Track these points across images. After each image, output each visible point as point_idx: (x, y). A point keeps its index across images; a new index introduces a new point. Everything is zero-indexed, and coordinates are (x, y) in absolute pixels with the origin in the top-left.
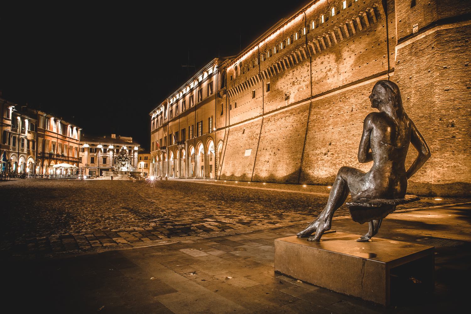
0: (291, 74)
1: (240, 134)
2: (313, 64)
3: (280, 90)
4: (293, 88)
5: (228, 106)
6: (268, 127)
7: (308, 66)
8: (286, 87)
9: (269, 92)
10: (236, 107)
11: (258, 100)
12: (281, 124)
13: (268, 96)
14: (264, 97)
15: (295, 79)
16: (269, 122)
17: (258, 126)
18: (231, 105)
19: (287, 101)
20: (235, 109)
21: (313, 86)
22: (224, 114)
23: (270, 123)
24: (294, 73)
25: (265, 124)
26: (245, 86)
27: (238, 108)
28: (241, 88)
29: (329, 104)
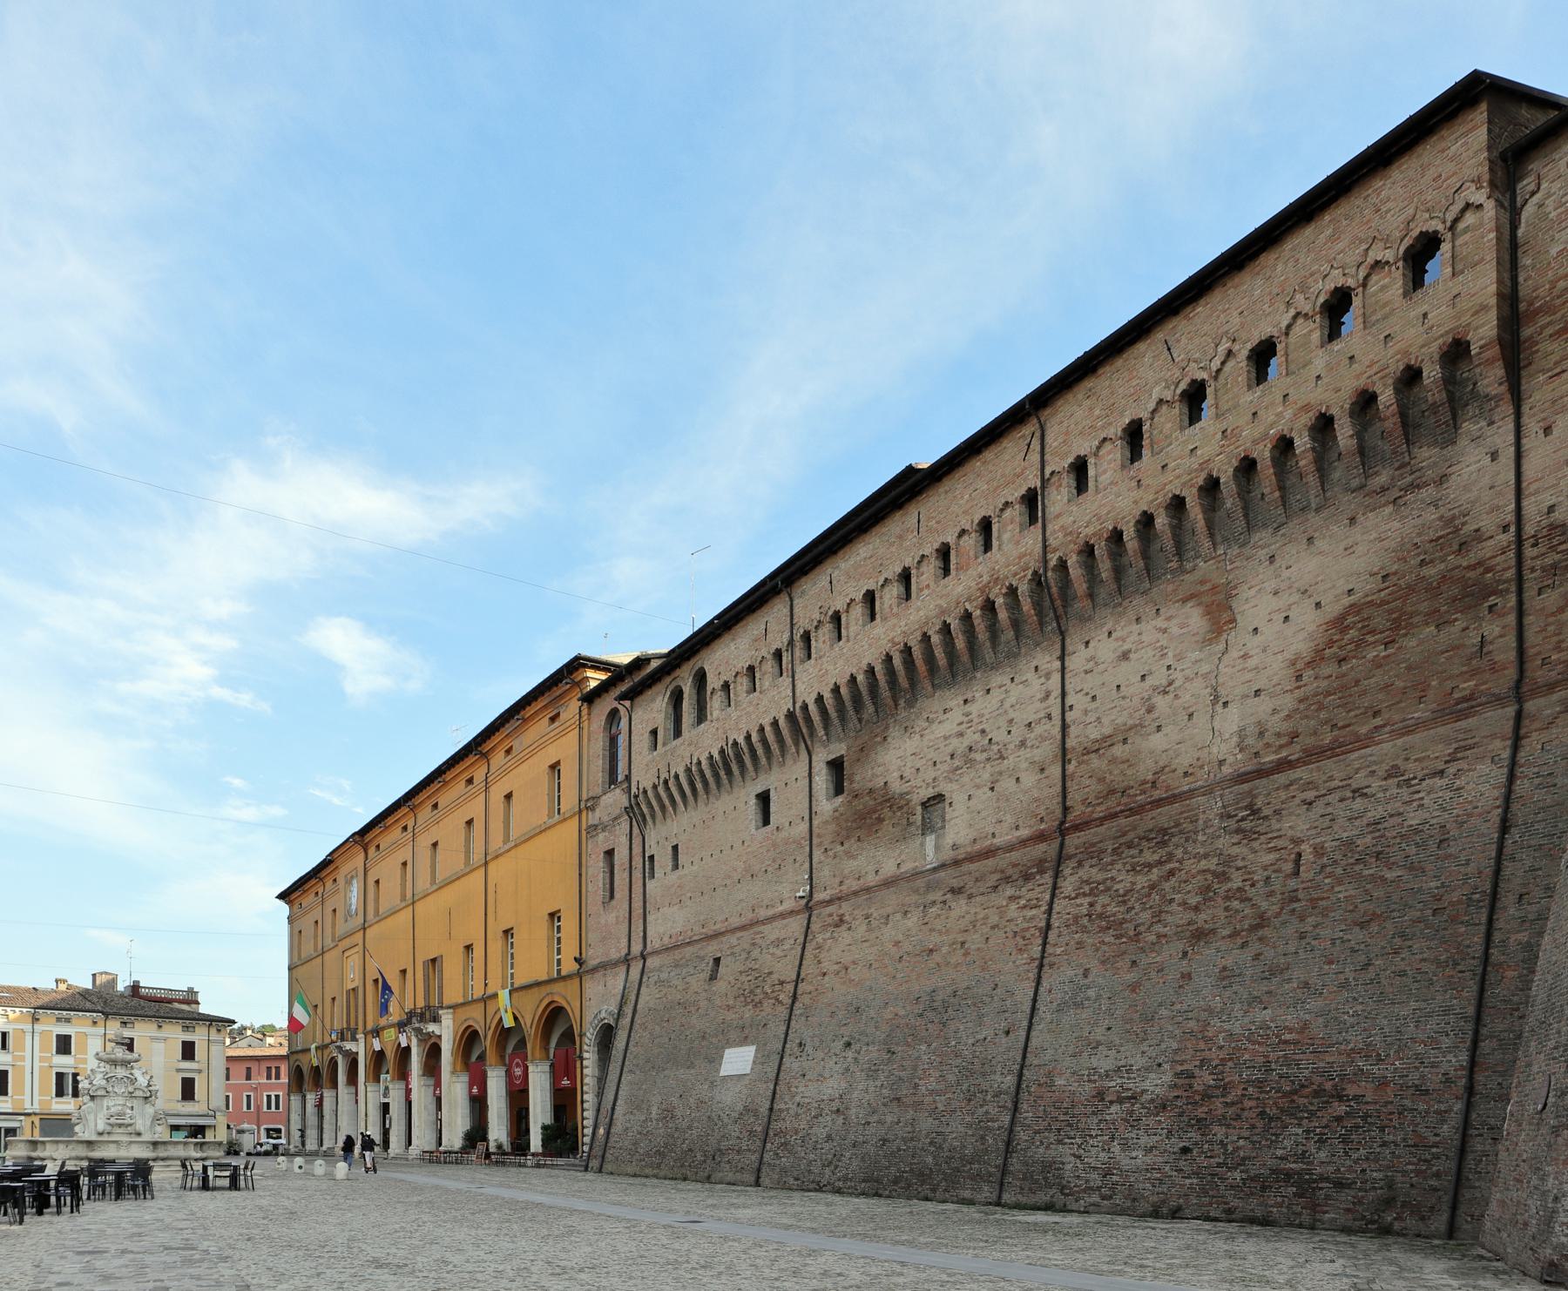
0: (956, 715)
1: (697, 981)
2: (1076, 662)
3: (896, 787)
4: (966, 779)
5: (638, 862)
6: (838, 948)
7: (1048, 676)
8: (930, 774)
9: (840, 799)
10: (676, 867)
11: (783, 834)
12: (900, 937)
13: (837, 817)
14: (815, 823)
15: (977, 736)
16: (845, 927)
17: (786, 947)
18: (652, 857)
19: (930, 840)
20: (674, 877)
21: (1071, 768)
22: (617, 895)
23: (844, 936)
24: (973, 709)
25: (820, 938)
26: (722, 773)
27: (686, 871)
28: (699, 786)
29: (1164, 844)
